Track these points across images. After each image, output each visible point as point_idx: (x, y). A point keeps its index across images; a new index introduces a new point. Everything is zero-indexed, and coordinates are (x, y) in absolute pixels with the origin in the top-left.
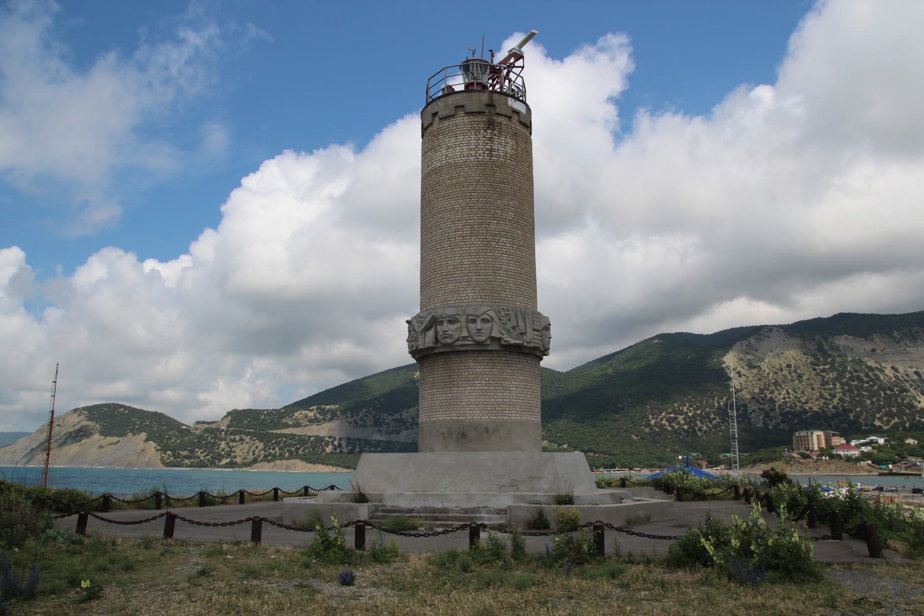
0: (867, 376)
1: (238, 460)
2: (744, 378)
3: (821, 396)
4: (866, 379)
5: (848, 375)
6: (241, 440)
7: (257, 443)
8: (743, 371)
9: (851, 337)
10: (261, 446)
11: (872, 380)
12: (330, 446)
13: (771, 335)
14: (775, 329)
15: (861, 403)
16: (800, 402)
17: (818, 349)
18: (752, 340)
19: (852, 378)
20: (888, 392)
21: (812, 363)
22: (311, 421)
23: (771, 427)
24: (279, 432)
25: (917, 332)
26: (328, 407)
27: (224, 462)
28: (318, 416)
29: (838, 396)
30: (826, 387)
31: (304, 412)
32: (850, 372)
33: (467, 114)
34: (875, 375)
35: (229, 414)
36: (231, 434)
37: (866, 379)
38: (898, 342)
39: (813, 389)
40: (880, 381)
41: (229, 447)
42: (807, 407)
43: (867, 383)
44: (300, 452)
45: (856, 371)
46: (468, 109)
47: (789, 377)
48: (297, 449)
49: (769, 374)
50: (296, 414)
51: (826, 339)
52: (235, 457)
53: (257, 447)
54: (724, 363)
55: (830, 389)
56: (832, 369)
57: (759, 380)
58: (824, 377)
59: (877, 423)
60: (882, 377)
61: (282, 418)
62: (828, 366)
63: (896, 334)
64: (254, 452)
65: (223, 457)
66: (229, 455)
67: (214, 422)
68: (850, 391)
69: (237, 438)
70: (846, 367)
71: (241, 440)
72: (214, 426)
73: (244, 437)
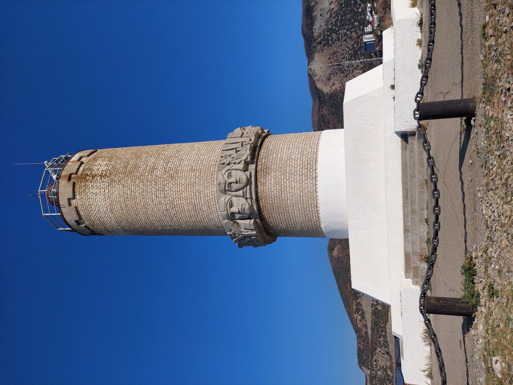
0: (334, 17)
1: (388, 364)
3: (345, 40)
4: (336, 18)
5: (334, 27)
6: (376, 361)
7: (377, 351)
8: (332, 82)
9: (314, 27)
10: (379, 349)
11: (337, 15)
12: (378, 307)
13: (313, 69)
14: (310, 67)
15: (349, 20)
18: (315, 79)
19: (336, 25)
20: (343, 6)
22: (363, 318)
23: (362, 66)
24: (370, 338)
26: (355, 307)
27: (389, 373)
29: (345, 31)
30: (340, 37)
31: (358, 322)
32: (332, 26)
33: (74, 197)
34: (334, 14)
35: (361, 368)
36: (373, 368)
37: (336, 18)
38: (317, 3)
40: (337, 11)
41: (380, 369)
42: (351, 48)
43: (338, 17)
44: (382, 325)
45: (332, 23)
46: (71, 196)
47: (335, 58)
48: (381, 327)
49: (333, 69)
50: (359, 326)
51: (315, 40)
53: (380, 352)
54: (327, 93)
55: (342, 36)
56: (330, 35)
57: (336, 74)
58: (335, 40)
59: (360, 10)
60: (335, 9)
61: (362, 336)
62: (330, 38)
63: (312, 4)
64: (383, 354)
65: (387, 373)
66: (385, 370)
67: (366, 377)
68: (343, 25)
70: (330, 29)
71: (376, 361)
72: (368, 378)
73: (374, 359)
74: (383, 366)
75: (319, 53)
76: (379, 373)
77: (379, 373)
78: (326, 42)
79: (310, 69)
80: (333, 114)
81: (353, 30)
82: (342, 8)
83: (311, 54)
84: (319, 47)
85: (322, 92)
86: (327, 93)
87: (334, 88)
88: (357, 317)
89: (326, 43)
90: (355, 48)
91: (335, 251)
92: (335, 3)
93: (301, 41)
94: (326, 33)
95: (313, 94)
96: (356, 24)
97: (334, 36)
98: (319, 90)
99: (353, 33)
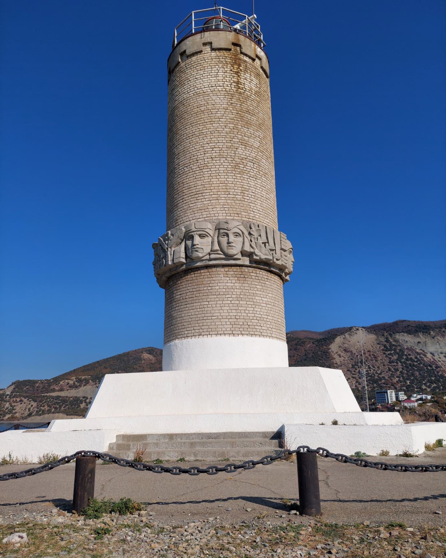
0: (416, 358)
2: (343, 358)
3: (390, 370)
4: (416, 360)
5: (405, 357)
6: (21, 401)
8: (342, 354)
9: (405, 334)
10: (35, 404)
11: (419, 360)
13: (358, 332)
14: (360, 329)
15: (413, 375)
16: (376, 373)
17: (386, 341)
19: (407, 359)
20: (429, 368)
21: (382, 350)
22: (71, 387)
23: (360, 389)
24: (48, 395)
25: (444, 332)
27: (8, 416)
28: (76, 383)
31: (66, 381)
32: (406, 355)
34: (420, 357)
35: (13, 384)
36: (14, 397)
37: (416, 360)
38: (433, 338)
39: (384, 365)
40: (424, 361)
41: (11, 406)
43: (417, 362)
44: (62, 408)
45: (409, 355)
47: (370, 358)
48: (60, 406)
49: (357, 356)
50: (61, 383)
51: (391, 335)
52: (16, 413)
54: (330, 349)
55: (394, 366)
56: (396, 353)
57: (351, 359)
58: (390, 358)
59: (424, 387)
60: (425, 359)
61: (51, 386)
62: (393, 352)
63: (432, 333)
65: (7, 413)
66: (10, 412)
68: (407, 367)
69: (18, 400)
70: (404, 352)
71: (21, 401)
73: (23, 399)
74: (15, 410)
75: (376, 340)
76: (7, 405)
77: (7, 405)
78: (388, 348)
79: (358, 329)
80: (305, 355)
81: (401, 379)
82: (426, 366)
83: (375, 331)
84: (382, 339)
85: (332, 343)
86: (330, 349)
87: (336, 356)
88: (72, 380)
89: (387, 348)
90: (381, 380)
91: (148, 355)
92: (433, 358)
93: (390, 320)
94: (399, 348)
95: (329, 332)
96: (408, 382)
97: (395, 357)
98: (334, 339)
99: (397, 379)
